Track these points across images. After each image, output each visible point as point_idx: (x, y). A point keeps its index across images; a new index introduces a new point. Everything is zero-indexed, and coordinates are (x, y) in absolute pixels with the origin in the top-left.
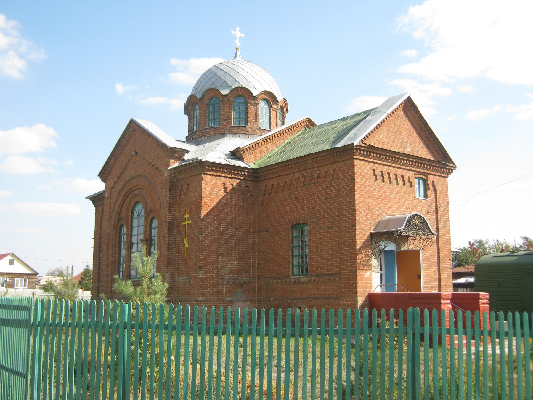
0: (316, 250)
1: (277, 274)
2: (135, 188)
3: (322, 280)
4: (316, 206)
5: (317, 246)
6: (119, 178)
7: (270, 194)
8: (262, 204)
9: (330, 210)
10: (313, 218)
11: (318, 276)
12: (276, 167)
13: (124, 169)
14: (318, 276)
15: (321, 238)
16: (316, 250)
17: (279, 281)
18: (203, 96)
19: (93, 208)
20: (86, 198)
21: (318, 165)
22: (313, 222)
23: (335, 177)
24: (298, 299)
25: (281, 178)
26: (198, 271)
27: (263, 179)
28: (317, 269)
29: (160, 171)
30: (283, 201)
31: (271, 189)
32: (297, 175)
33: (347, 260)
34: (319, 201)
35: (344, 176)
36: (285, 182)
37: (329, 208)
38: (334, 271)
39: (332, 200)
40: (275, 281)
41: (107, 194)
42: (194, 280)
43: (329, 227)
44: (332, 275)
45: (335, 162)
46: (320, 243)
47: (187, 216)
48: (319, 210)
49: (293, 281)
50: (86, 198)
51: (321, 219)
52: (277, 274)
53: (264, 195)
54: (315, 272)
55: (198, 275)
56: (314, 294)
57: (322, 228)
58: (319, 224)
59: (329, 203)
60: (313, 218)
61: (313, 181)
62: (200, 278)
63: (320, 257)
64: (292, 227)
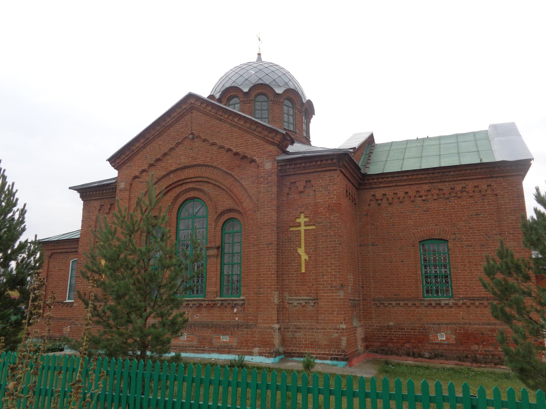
0: (462, 270)
1: (395, 295)
2: (188, 181)
3: (477, 303)
4: (460, 221)
5: (465, 265)
6: (151, 165)
7: (379, 204)
8: (367, 215)
9: (484, 227)
10: (455, 234)
12: (396, 175)
13: (165, 154)
14: (469, 299)
15: (471, 257)
16: (462, 270)
17: (402, 303)
18: (250, 90)
19: (80, 203)
20: (70, 188)
21: (463, 178)
22: (454, 239)
23: (489, 192)
24: (438, 324)
25: (399, 188)
26: (339, 290)
27: (369, 187)
28: (466, 291)
29: (253, 161)
30: (401, 213)
31: (382, 200)
32: (426, 187)
35: (507, 193)
36: (407, 193)
37: (482, 225)
39: (487, 217)
40: (394, 303)
41: (122, 185)
42: (327, 302)
43: (483, 245)
45: (492, 177)
46: (469, 262)
47: (302, 220)
48: (465, 226)
49: (426, 303)
50: (70, 188)
51: (469, 236)
52: (395, 295)
53: (369, 205)
54: (463, 294)
55: (339, 296)
56: (463, 319)
57: (471, 246)
58: (465, 241)
59: (481, 220)
60: (455, 234)
61: (453, 195)
62: (342, 299)
63: (471, 278)
64: (419, 242)
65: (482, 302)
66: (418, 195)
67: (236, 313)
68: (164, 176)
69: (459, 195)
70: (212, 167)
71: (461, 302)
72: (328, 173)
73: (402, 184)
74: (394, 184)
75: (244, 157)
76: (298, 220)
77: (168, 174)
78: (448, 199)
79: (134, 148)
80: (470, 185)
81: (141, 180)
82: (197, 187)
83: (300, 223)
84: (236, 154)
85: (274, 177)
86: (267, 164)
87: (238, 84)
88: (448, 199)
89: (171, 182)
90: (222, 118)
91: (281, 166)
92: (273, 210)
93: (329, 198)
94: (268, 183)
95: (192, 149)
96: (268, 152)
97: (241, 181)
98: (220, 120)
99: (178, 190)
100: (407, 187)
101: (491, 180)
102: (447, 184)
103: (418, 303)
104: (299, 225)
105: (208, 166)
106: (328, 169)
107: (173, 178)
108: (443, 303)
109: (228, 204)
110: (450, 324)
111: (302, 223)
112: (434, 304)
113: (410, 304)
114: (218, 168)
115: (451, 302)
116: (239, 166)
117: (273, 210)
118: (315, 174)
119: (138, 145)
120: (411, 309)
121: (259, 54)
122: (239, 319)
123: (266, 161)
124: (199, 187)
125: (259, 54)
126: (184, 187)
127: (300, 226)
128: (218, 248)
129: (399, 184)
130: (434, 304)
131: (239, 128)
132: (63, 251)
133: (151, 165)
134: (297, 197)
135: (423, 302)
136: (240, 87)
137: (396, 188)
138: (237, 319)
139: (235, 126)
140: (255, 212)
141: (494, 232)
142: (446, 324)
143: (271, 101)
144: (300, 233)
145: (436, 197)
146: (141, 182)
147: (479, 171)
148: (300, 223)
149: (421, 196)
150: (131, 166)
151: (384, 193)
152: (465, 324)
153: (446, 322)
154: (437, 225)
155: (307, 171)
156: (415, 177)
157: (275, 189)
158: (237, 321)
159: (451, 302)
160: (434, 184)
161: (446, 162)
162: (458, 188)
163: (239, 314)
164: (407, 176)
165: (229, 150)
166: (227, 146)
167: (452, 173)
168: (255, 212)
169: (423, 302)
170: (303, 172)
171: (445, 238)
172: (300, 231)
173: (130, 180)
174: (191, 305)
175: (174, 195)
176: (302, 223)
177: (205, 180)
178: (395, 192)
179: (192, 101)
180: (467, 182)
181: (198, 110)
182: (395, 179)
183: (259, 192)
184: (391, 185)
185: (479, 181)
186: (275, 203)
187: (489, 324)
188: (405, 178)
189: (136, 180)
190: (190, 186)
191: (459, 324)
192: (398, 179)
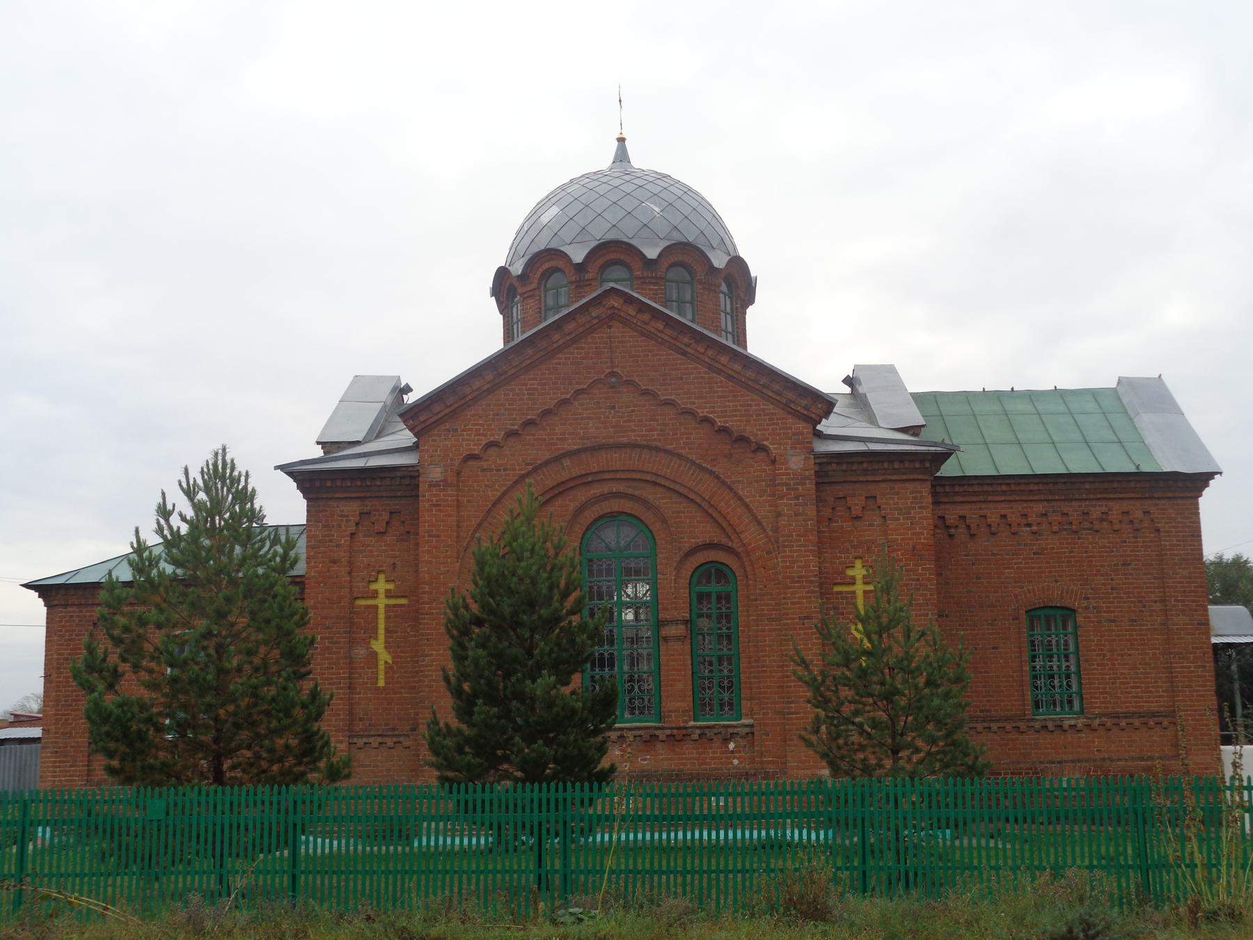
2: (607, 476)
5: (1104, 656)
7: (951, 536)
11: (1116, 716)
13: (547, 413)
17: (994, 726)
18: (660, 255)
22: (1087, 608)
24: (1059, 762)
32: (1040, 508)
33: (1190, 686)
34: (1103, 566)
36: (1004, 516)
38: (1154, 707)
40: (980, 726)
44: (1153, 715)
46: (1111, 651)
47: (858, 571)
48: (1104, 584)
49: (1037, 725)
50: (277, 468)
65: (1131, 721)
66: (1024, 521)
67: (732, 752)
68: (547, 463)
69: (1096, 527)
70: (666, 451)
71: (1097, 721)
72: (909, 485)
73: (996, 498)
74: (982, 498)
75: (742, 439)
76: (850, 572)
77: (558, 459)
78: (1076, 532)
79: (468, 390)
80: (1116, 509)
81: (485, 464)
82: (630, 491)
83: (853, 578)
84: (724, 430)
85: (810, 485)
86: (794, 459)
87: (627, 233)
88: (1076, 532)
89: (565, 475)
90: (688, 349)
91: (820, 464)
92: (810, 551)
93: (914, 534)
94: (797, 498)
95: (613, 407)
96: (794, 434)
97: (734, 487)
98: (684, 353)
99: (582, 495)
100: (1003, 505)
101: (1150, 502)
102: (1075, 504)
103: (1023, 726)
104: (852, 582)
105: (657, 449)
106: (912, 477)
107: (570, 469)
108: (1066, 724)
109: (705, 532)
110: (1078, 761)
111: (859, 577)
112: (1051, 727)
113: (1009, 727)
114: (680, 456)
115: (1081, 722)
116: (729, 457)
117: (810, 551)
118: (884, 485)
119: (477, 384)
120: (1010, 736)
121: (621, 140)
122: (741, 763)
123: (792, 452)
124: (636, 493)
125: (621, 140)
126: (595, 491)
127: (854, 584)
128: (686, 622)
129: (990, 498)
130: (1050, 725)
131: (729, 377)
133: (511, 434)
134: (847, 526)
135: (1031, 724)
136: (633, 242)
137: (983, 506)
138: (736, 762)
139: (719, 372)
140: (769, 553)
141: (1153, 597)
142: (1072, 761)
143: (700, 282)
144: (855, 598)
145: (1055, 528)
146: (484, 470)
147: (1133, 484)
148: (853, 578)
149: (1029, 525)
150: (456, 430)
151: (962, 513)
152: (1104, 759)
153: (1071, 757)
154: (1056, 581)
155: (869, 478)
156: (1022, 487)
157: (811, 511)
158: (735, 768)
159: (1081, 722)
160: (1055, 504)
161: (1080, 463)
162: (1096, 513)
163: (739, 752)
164: (1009, 484)
165: (706, 420)
166: (702, 413)
167: (1087, 486)
168: (769, 553)
169: (1031, 724)
170: (862, 479)
171: (1071, 606)
172: (854, 592)
173: (457, 463)
174: (390, 744)
175: (572, 506)
176: (859, 577)
177: (649, 477)
178: (982, 513)
180: (1110, 503)
181: (625, 322)
182: (986, 488)
183: (779, 515)
184: (975, 499)
185: (1131, 502)
186: (813, 537)
187: (1142, 759)
188: (1004, 488)
189: (471, 463)
190: (606, 488)
191: (1095, 760)
192: (990, 489)
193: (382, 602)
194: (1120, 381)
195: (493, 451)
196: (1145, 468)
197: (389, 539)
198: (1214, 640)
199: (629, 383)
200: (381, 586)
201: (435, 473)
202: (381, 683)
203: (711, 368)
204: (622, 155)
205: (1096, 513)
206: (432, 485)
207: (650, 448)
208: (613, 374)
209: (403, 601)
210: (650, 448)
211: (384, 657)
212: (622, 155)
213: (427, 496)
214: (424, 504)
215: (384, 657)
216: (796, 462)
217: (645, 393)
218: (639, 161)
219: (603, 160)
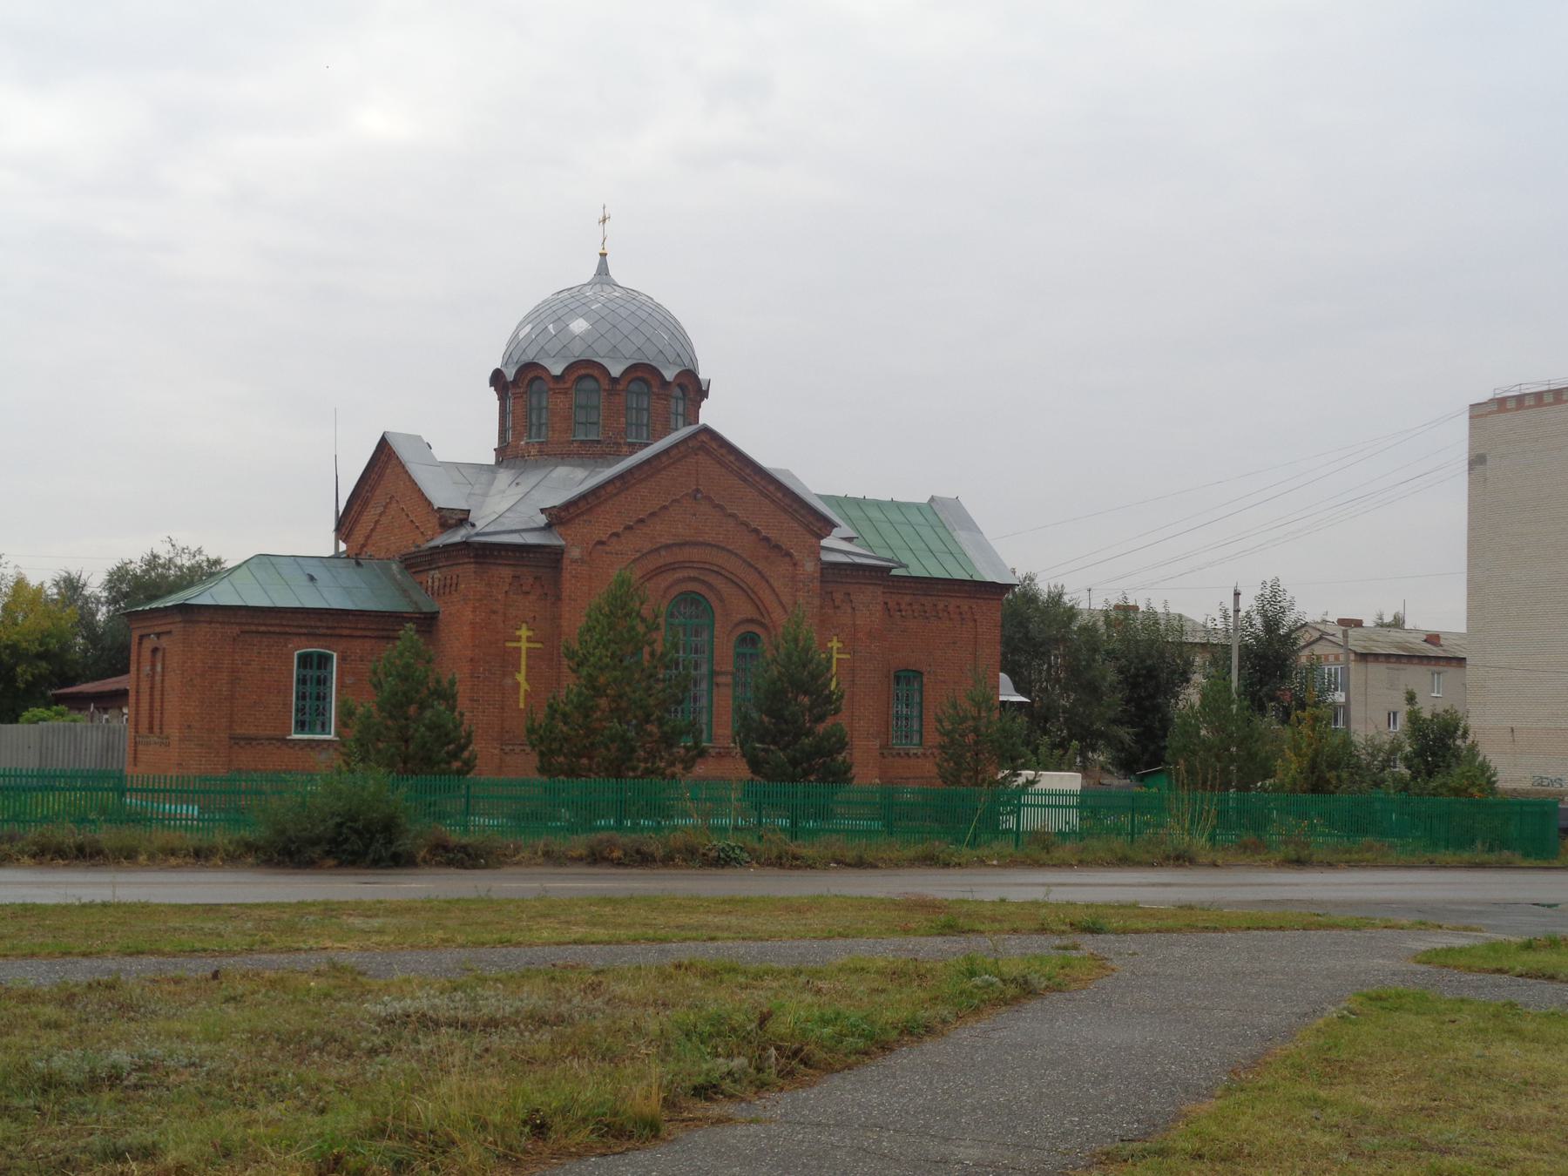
13: (653, 514)
29: (788, 554)
32: (908, 599)
75: (777, 547)
77: (657, 550)
84: (767, 539)
89: (661, 562)
98: (745, 480)
105: (723, 549)
107: (665, 558)
109: (748, 611)
115: (920, 752)
121: (603, 255)
125: (603, 255)
126: (679, 575)
128: (732, 674)
131: (773, 501)
132: (277, 629)
133: (629, 528)
139: (767, 497)
157: (817, 602)
159: (920, 752)
162: (941, 606)
165: (756, 531)
166: (754, 525)
179: (703, 437)
181: (708, 452)
193: (524, 645)
194: (932, 499)
195: (614, 539)
196: (976, 578)
197: (532, 597)
198: (1002, 698)
199: (708, 498)
200: (524, 632)
201: (575, 553)
202: (522, 706)
203: (761, 492)
204: (603, 270)
205: (941, 606)
206: (574, 561)
207: (718, 547)
208: (697, 490)
209: (539, 645)
210: (718, 547)
211: (524, 686)
212: (603, 270)
213: (568, 570)
214: (566, 575)
215: (524, 686)
216: (810, 567)
217: (717, 506)
218: (614, 273)
219: (589, 272)
